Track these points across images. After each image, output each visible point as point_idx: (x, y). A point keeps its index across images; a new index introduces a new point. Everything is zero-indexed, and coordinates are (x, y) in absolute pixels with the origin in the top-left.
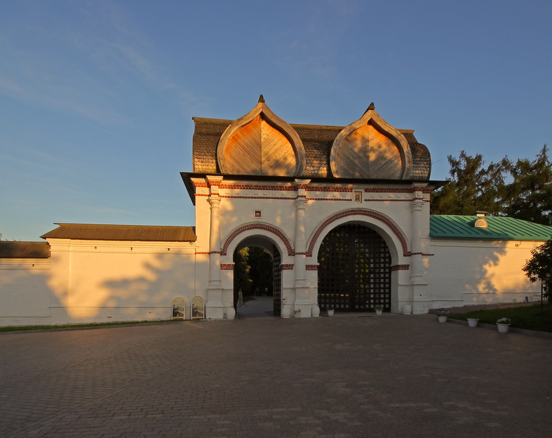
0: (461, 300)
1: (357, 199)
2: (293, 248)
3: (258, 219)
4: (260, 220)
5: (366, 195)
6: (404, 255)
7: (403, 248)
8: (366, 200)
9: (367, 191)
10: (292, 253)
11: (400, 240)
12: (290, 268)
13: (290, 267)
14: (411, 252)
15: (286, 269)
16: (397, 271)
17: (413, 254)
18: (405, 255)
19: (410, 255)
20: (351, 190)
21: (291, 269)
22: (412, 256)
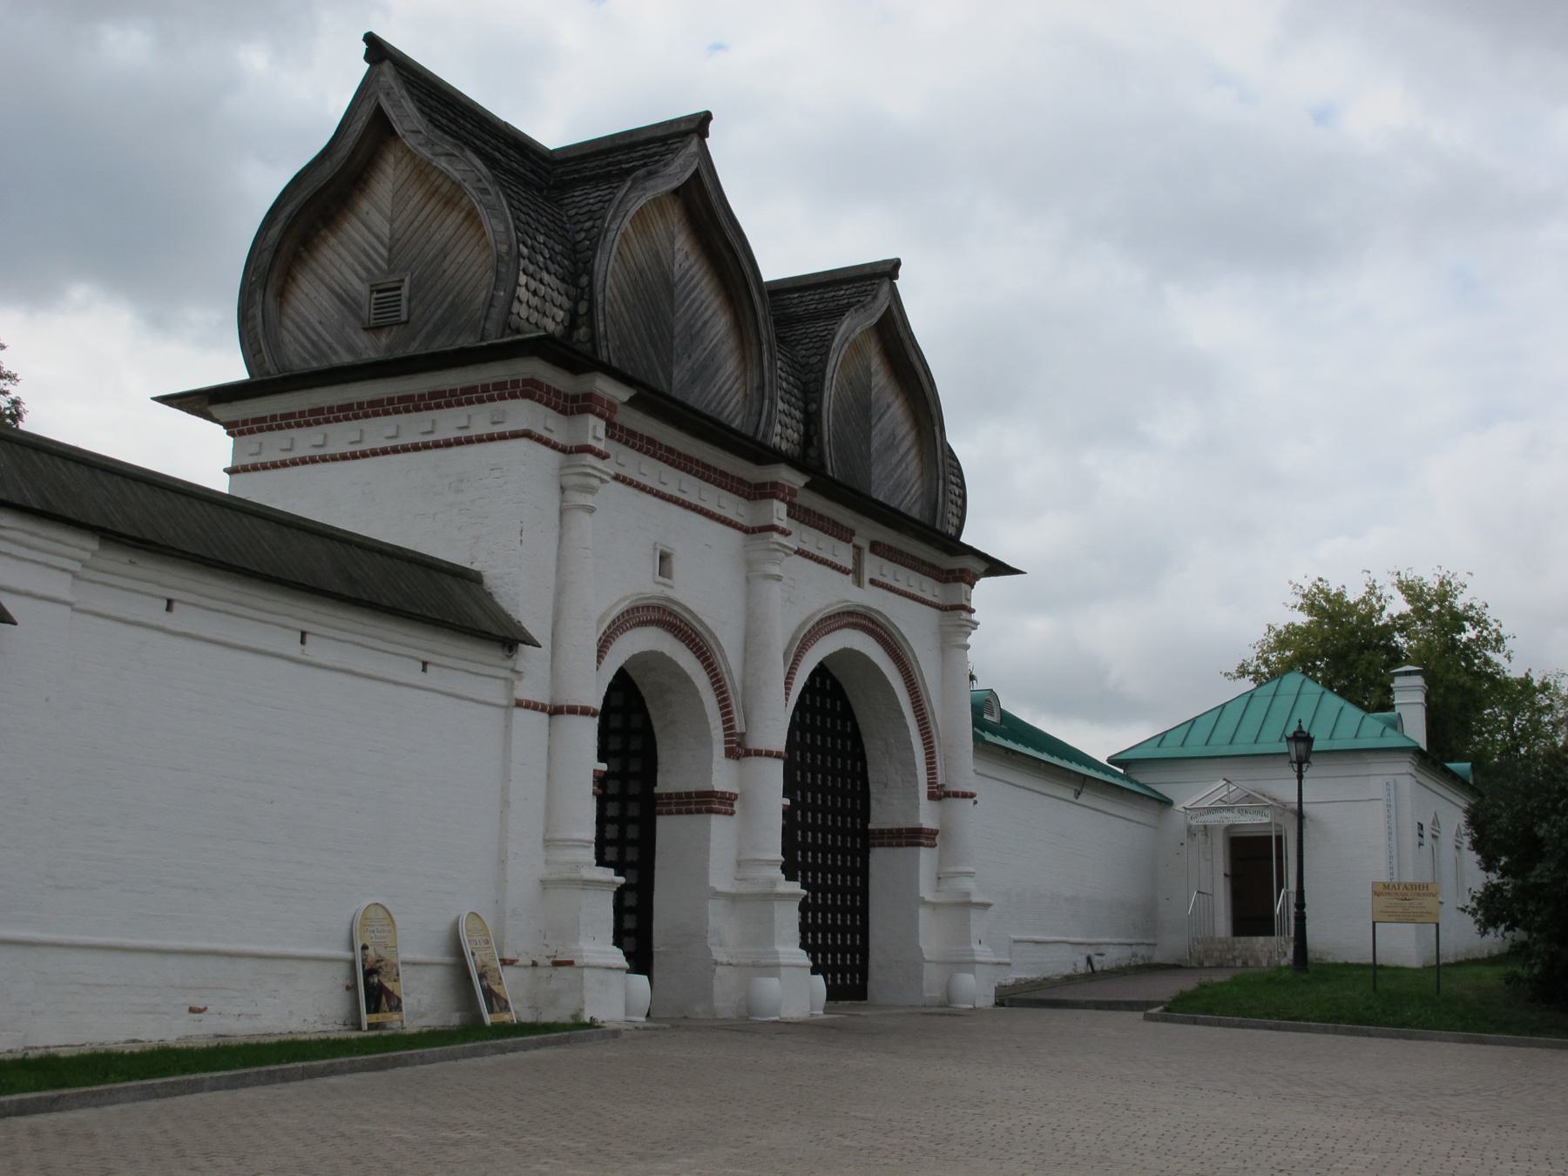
0: (1007, 960)
1: (856, 573)
2: (739, 727)
3: (663, 588)
4: (669, 593)
5: (873, 566)
6: (929, 792)
7: (928, 769)
8: (873, 582)
9: (875, 548)
10: (738, 749)
11: (923, 740)
12: (673, 808)
13: (707, 802)
14: (943, 786)
15: (718, 812)
16: (914, 849)
17: (947, 795)
18: (931, 796)
19: (939, 798)
20: (843, 533)
21: (726, 813)
22: (948, 800)
